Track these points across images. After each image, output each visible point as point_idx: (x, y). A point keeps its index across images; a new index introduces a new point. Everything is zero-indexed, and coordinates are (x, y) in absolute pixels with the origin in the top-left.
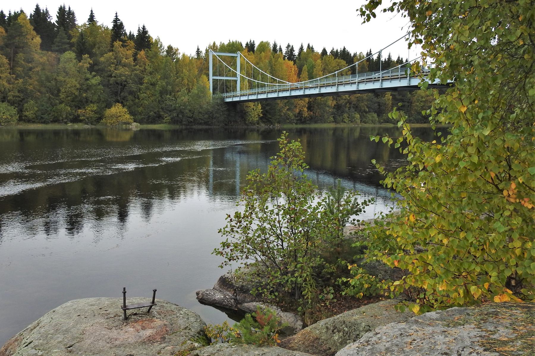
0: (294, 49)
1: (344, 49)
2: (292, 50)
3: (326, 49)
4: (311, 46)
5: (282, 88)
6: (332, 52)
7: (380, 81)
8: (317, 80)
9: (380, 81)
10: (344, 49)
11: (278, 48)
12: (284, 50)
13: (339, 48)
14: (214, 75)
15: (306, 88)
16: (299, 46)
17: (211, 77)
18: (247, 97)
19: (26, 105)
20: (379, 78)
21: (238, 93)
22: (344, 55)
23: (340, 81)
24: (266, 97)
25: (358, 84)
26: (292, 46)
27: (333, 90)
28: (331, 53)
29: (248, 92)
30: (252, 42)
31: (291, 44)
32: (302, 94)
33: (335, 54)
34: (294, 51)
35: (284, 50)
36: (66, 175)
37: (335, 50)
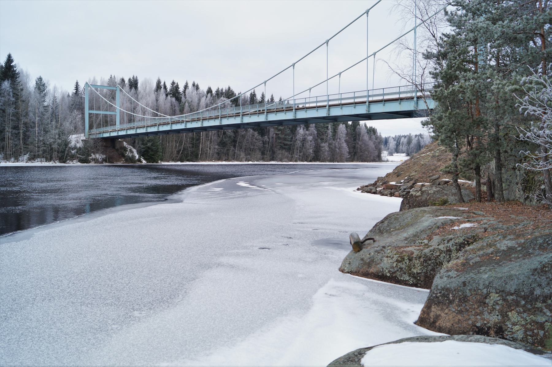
0: (179, 86)
1: (229, 88)
2: (177, 87)
3: (212, 89)
4: (196, 84)
5: (162, 121)
6: (217, 91)
7: (265, 113)
8: (183, 116)
9: (265, 113)
10: (229, 88)
11: (162, 84)
12: (169, 87)
13: (224, 87)
14: (91, 108)
15: (204, 119)
16: (184, 84)
17: (87, 112)
18: (125, 131)
19: (179, 90)
20: (264, 110)
21: (118, 126)
22: (229, 94)
23: (223, 114)
24: (156, 131)
25: (242, 117)
26: (177, 83)
27: (216, 123)
28: (216, 92)
29: (126, 126)
30: (135, 77)
31: (176, 81)
32: (169, 129)
33: (219, 94)
34: (179, 89)
35: (169, 87)
36: (307, 228)
37: (220, 89)
